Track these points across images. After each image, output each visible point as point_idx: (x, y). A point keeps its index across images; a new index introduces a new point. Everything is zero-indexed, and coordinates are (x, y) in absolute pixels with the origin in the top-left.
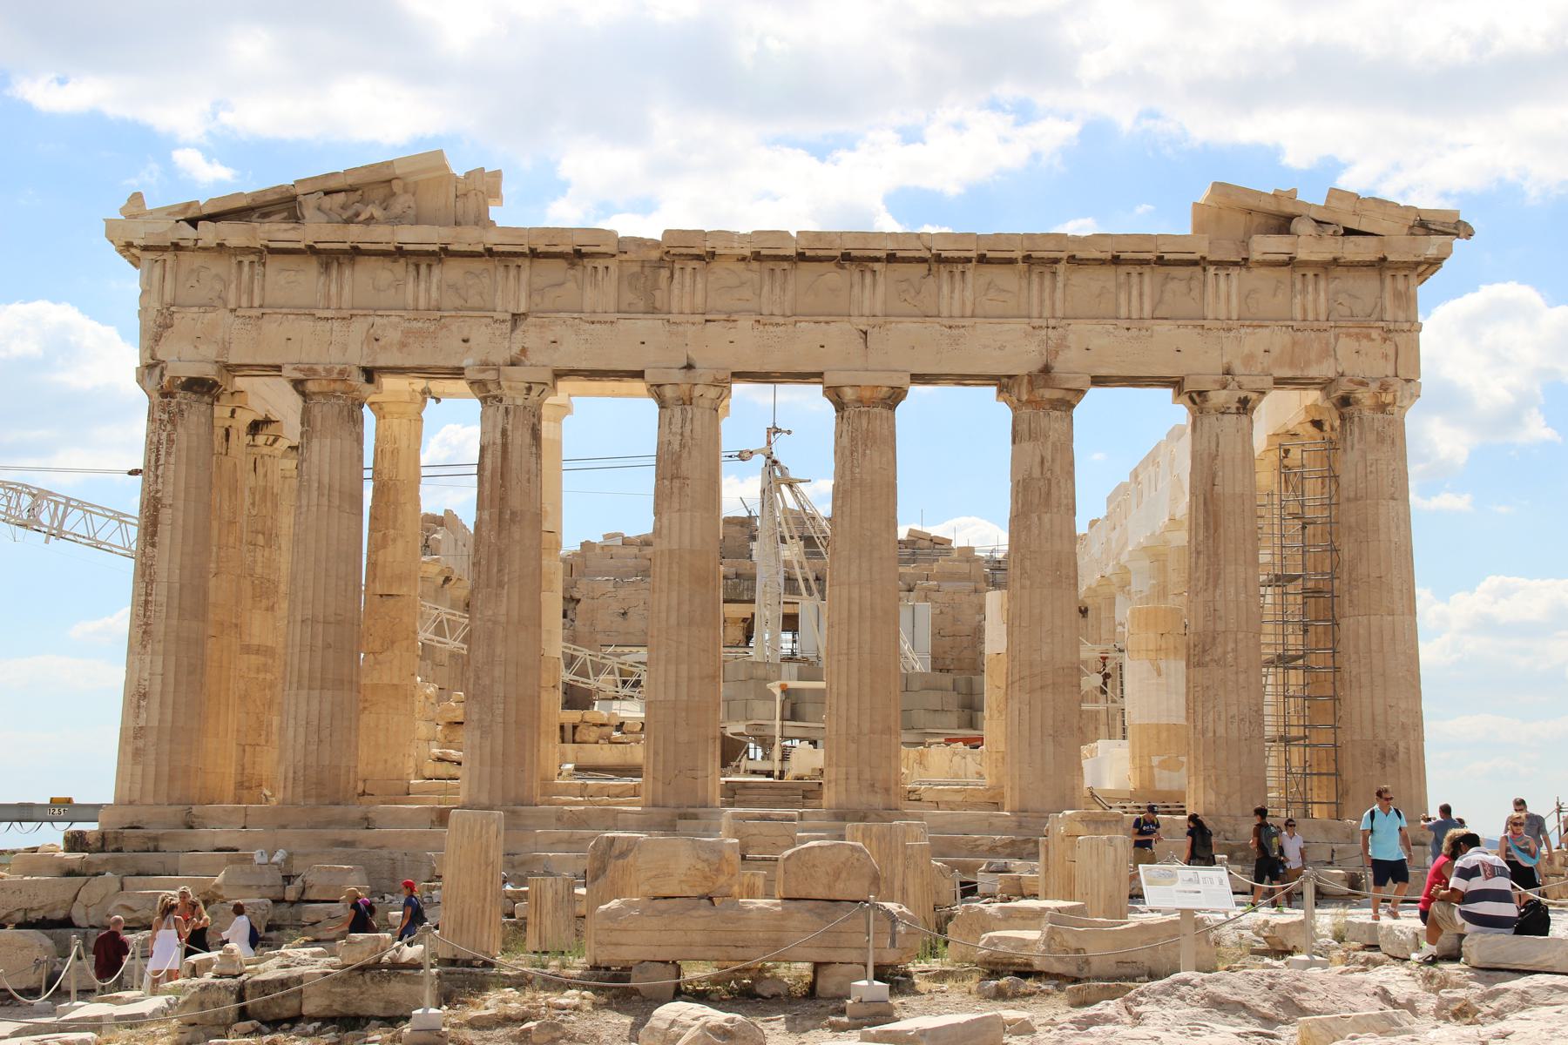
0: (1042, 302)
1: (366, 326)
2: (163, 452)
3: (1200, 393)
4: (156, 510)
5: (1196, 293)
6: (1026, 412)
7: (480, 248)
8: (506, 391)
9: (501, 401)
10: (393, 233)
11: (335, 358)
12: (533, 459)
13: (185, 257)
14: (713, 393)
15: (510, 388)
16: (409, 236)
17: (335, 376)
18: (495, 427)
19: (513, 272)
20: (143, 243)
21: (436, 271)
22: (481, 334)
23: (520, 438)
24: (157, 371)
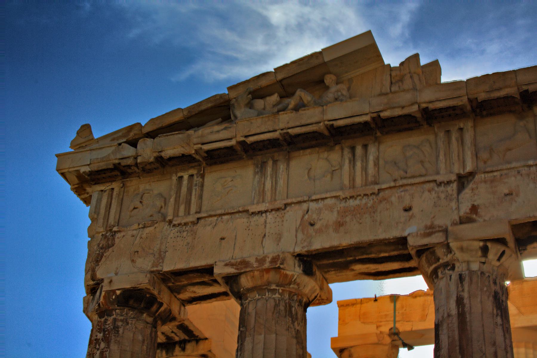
1: (300, 213)
7: (415, 108)
8: (458, 255)
9: (453, 268)
10: (323, 112)
11: (270, 249)
12: (499, 332)
13: (133, 184)
15: (462, 249)
16: (339, 113)
17: (267, 265)
19: (454, 136)
21: (372, 150)
23: (480, 306)
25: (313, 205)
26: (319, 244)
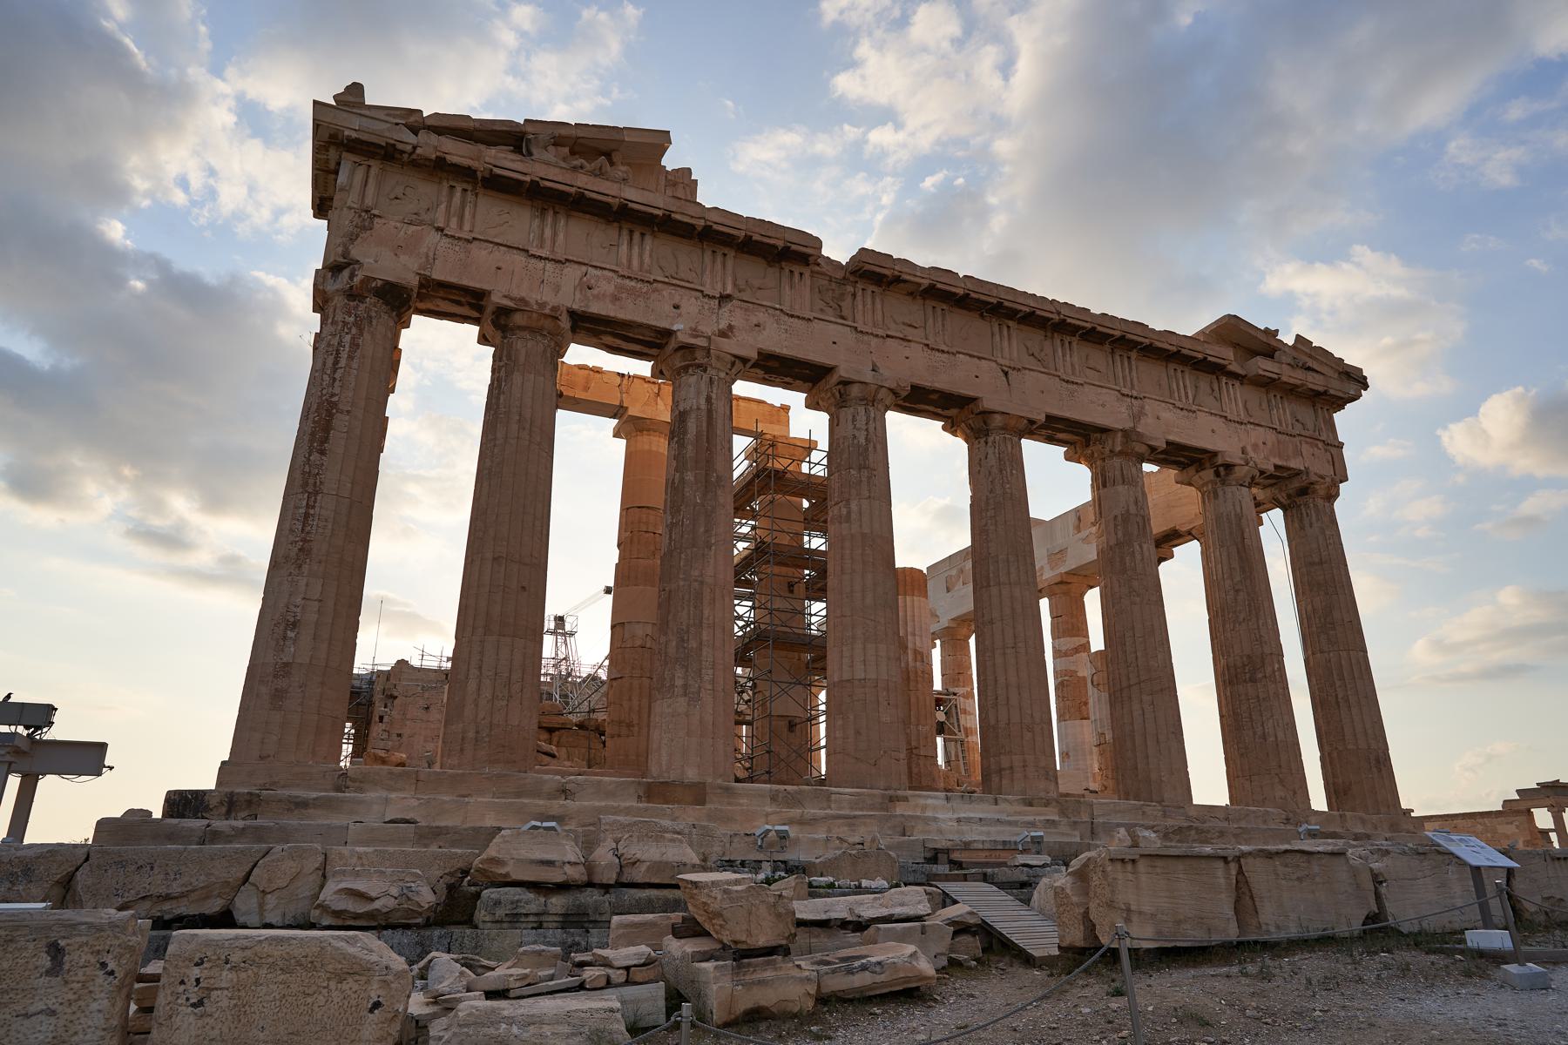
0: (1124, 378)
2: (344, 355)
3: (1229, 467)
4: (331, 415)
5: (1217, 393)
6: (1117, 462)
7: (702, 223)
8: (714, 362)
11: (549, 298)
14: (890, 399)
15: (718, 358)
17: (547, 311)
18: (698, 393)
19: (719, 259)
20: (354, 135)
22: (691, 305)
24: (346, 273)
25: (592, 271)
26: (595, 308)
